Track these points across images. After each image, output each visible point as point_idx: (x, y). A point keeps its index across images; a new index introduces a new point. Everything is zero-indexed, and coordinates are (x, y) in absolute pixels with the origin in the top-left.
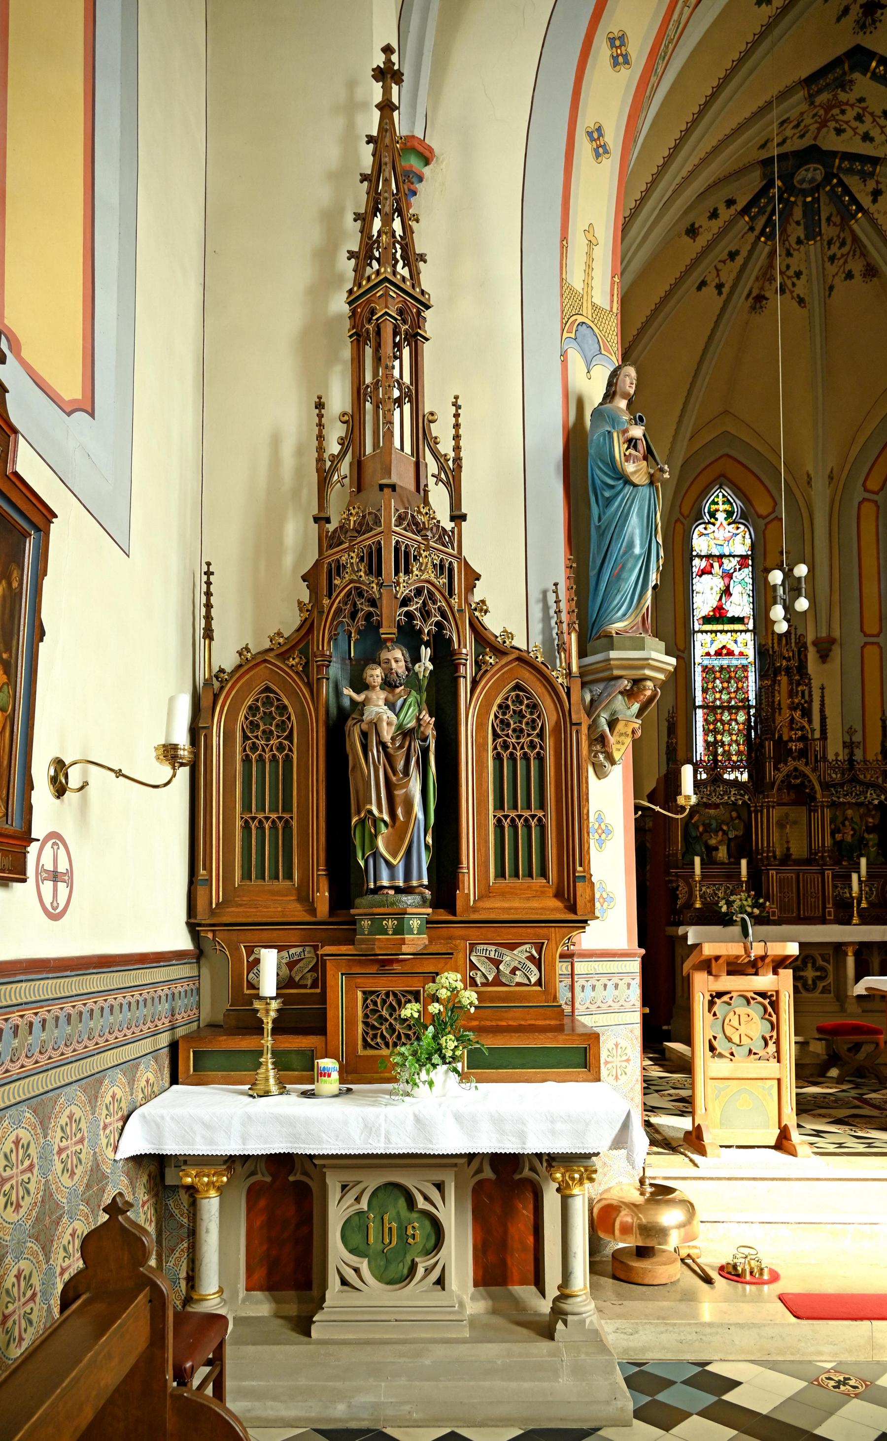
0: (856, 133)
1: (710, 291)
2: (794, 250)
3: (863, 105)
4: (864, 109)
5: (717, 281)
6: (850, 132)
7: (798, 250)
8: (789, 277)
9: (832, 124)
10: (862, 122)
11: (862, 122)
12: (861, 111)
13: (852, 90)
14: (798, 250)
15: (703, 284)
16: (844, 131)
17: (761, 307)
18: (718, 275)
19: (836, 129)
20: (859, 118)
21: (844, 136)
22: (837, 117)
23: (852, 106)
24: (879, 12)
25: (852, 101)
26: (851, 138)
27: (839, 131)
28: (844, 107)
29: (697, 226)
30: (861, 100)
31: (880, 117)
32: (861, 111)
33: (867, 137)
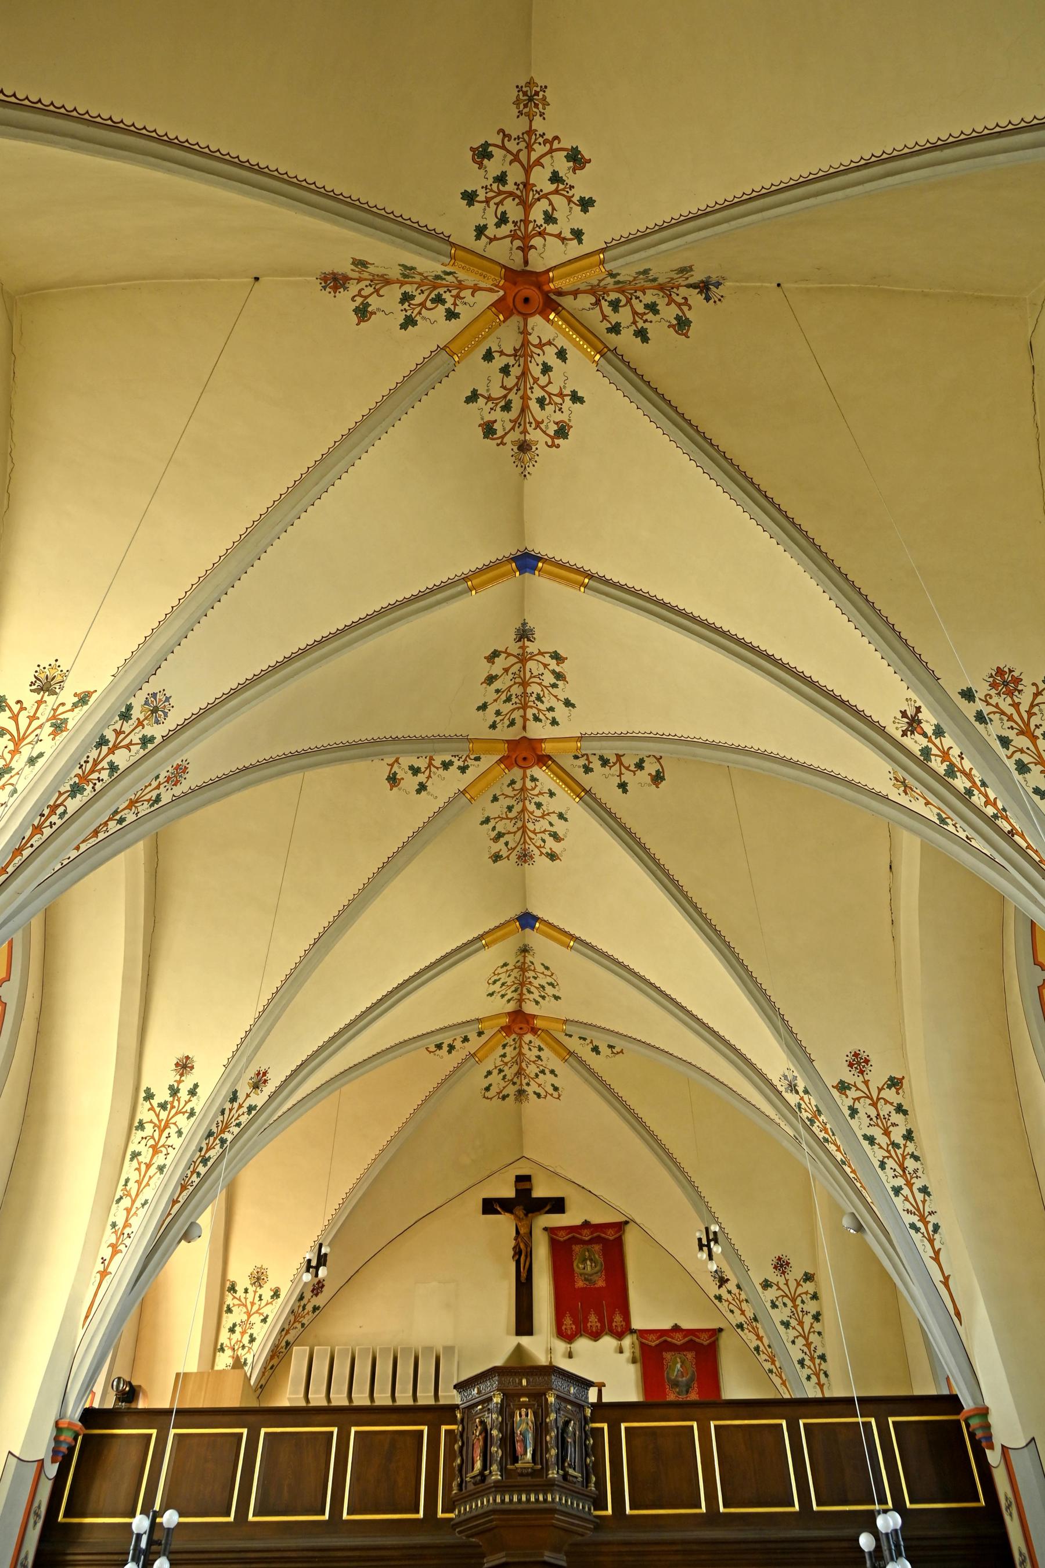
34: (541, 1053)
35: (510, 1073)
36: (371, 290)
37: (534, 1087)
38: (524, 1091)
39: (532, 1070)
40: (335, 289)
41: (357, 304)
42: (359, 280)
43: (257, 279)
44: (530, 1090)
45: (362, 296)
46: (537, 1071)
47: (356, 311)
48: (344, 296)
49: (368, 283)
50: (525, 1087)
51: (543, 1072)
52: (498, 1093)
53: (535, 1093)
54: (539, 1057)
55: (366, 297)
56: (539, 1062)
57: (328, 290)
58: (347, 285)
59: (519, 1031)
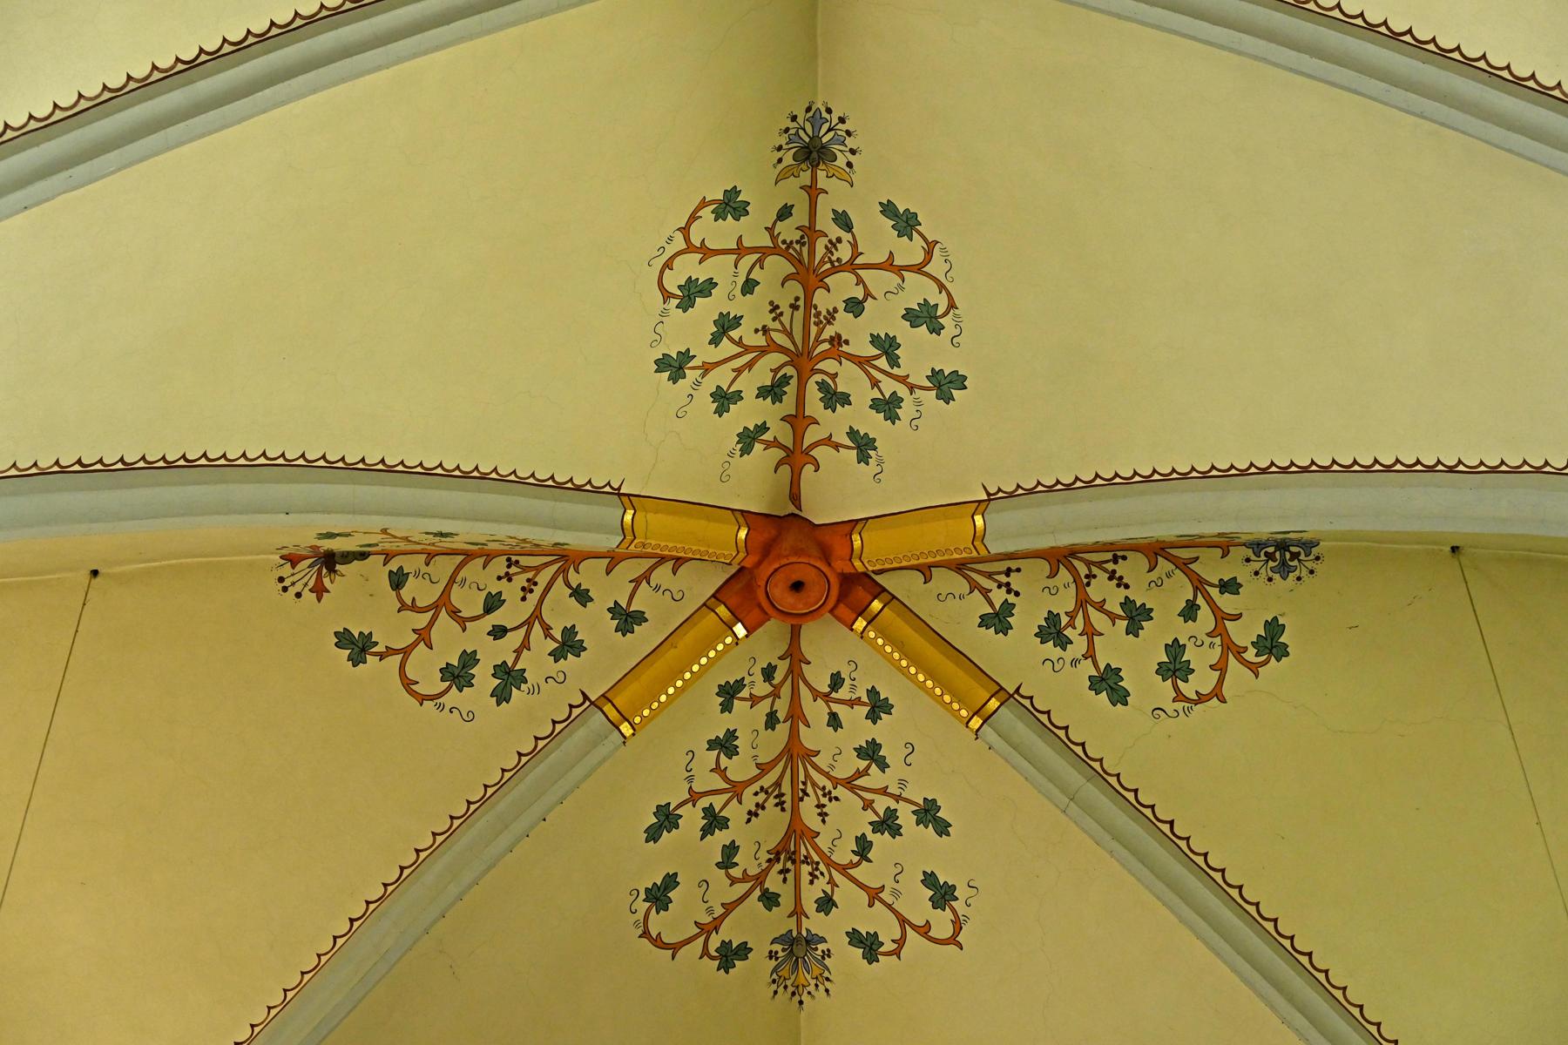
34: (881, 731)
35: (755, 837)
37: (853, 911)
38: (812, 940)
39: (845, 821)
44: (831, 929)
46: (862, 823)
50: (815, 923)
51: (888, 825)
52: (706, 930)
53: (855, 938)
54: (871, 752)
56: (875, 778)
59: (788, 600)
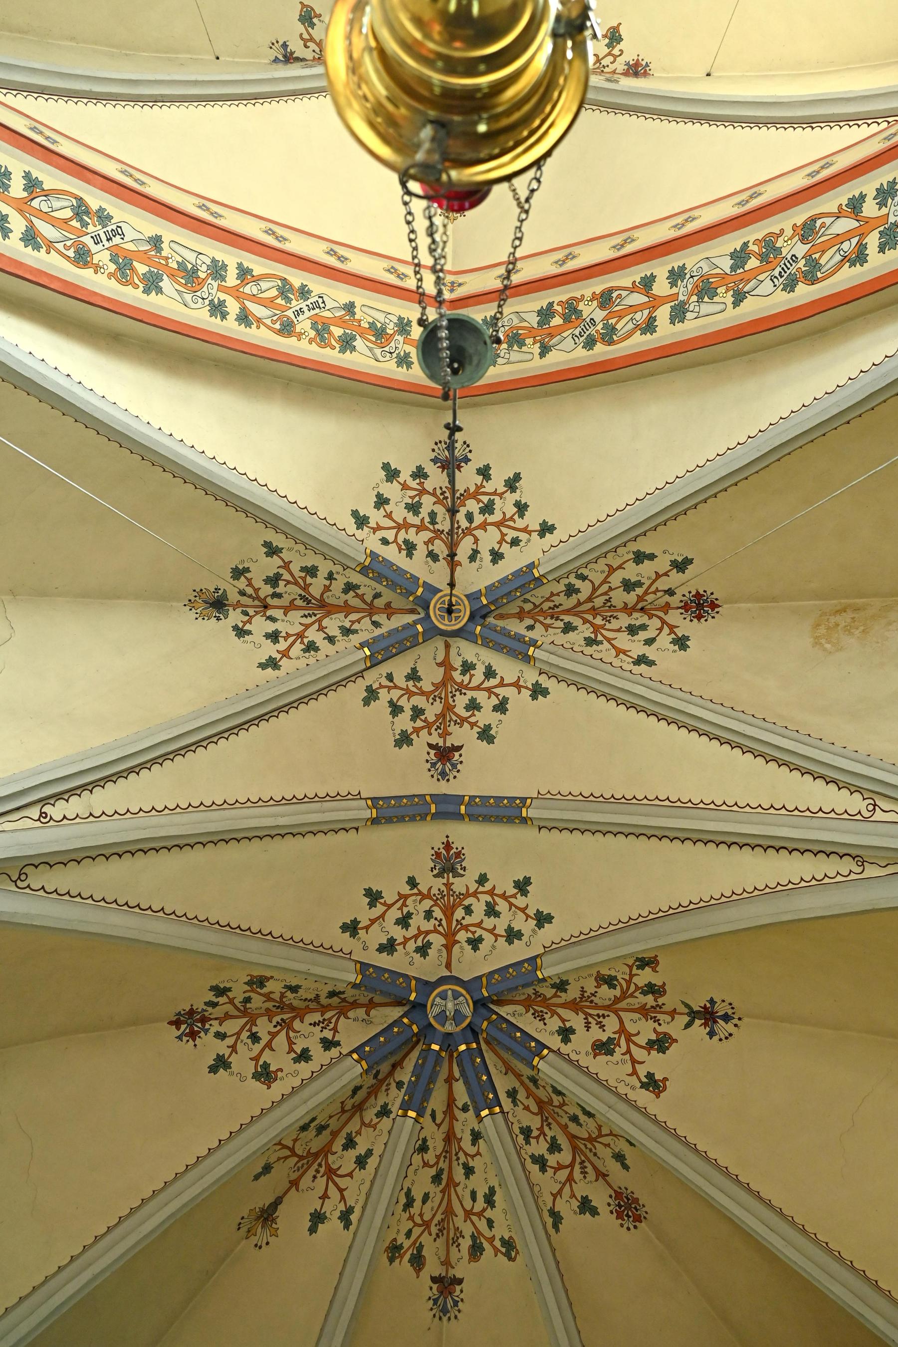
0: (496, 936)
1: (333, 1224)
2: (473, 1157)
3: (488, 886)
4: (491, 892)
5: (342, 1207)
6: (488, 938)
7: (478, 1153)
8: (480, 1214)
9: (462, 936)
10: (497, 914)
11: (497, 914)
12: (489, 898)
13: (464, 869)
14: (478, 1153)
15: (318, 1218)
16: (480, 940)
17: (456, 1303)
18: (343, 1198)
19: (470, 941)
20: (491, 911)
21: (484, 947)
22: (464, 922)
23: (475, 894)
24: (457, 754)
25: (473, 887)
26: (494, 947)
27: (475, 943)
28: (466, 902)
29: (273, 1068)
30: (482, 879)
31: (514, 896)
32: (489, 899)
33: (512, 935)
36: (604, 62)
40: (637, 64)
41: (619, 47)
42: (614, 72)
43: (708, 75)
45: (613, 55)
47: (619, 40)
48: (629, 56)
49: (606, 70)
55: (609, 54)
57: (644, 63)
58: (626, 67)
